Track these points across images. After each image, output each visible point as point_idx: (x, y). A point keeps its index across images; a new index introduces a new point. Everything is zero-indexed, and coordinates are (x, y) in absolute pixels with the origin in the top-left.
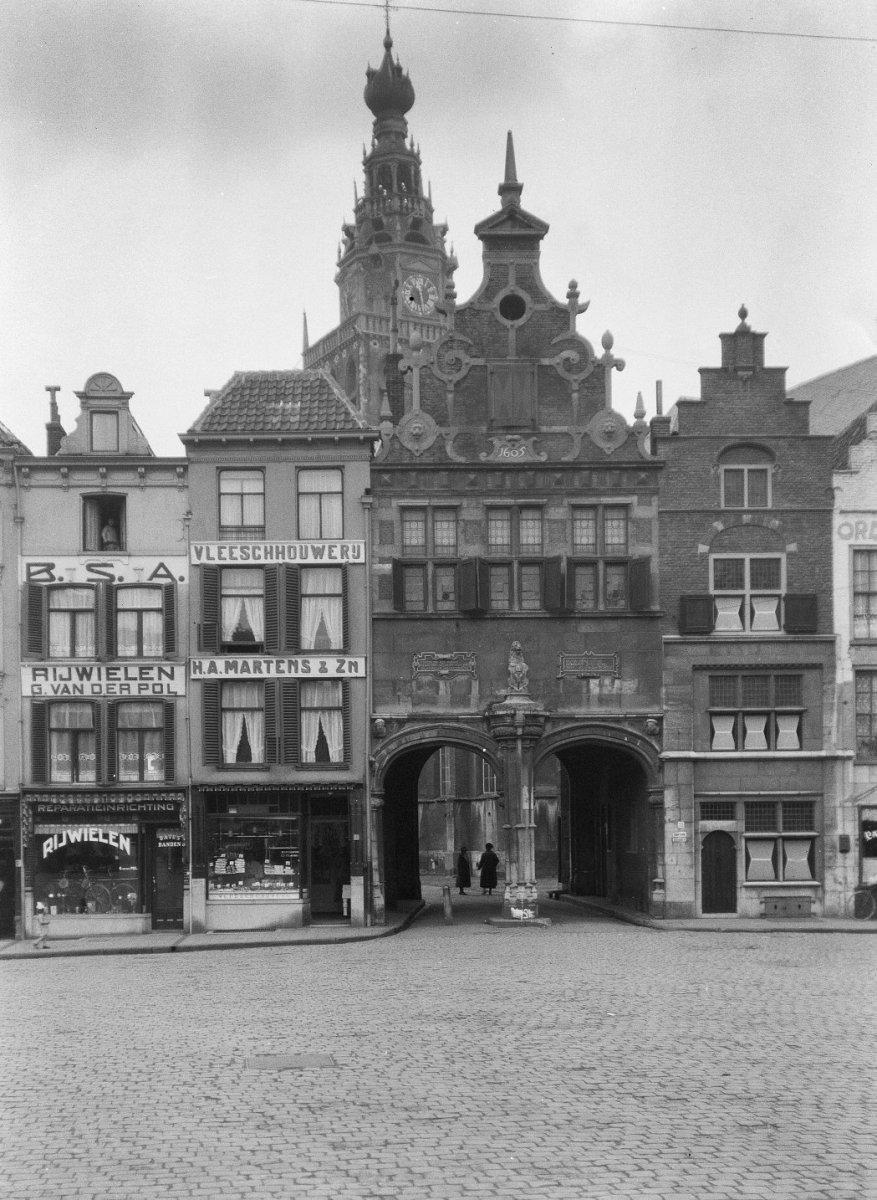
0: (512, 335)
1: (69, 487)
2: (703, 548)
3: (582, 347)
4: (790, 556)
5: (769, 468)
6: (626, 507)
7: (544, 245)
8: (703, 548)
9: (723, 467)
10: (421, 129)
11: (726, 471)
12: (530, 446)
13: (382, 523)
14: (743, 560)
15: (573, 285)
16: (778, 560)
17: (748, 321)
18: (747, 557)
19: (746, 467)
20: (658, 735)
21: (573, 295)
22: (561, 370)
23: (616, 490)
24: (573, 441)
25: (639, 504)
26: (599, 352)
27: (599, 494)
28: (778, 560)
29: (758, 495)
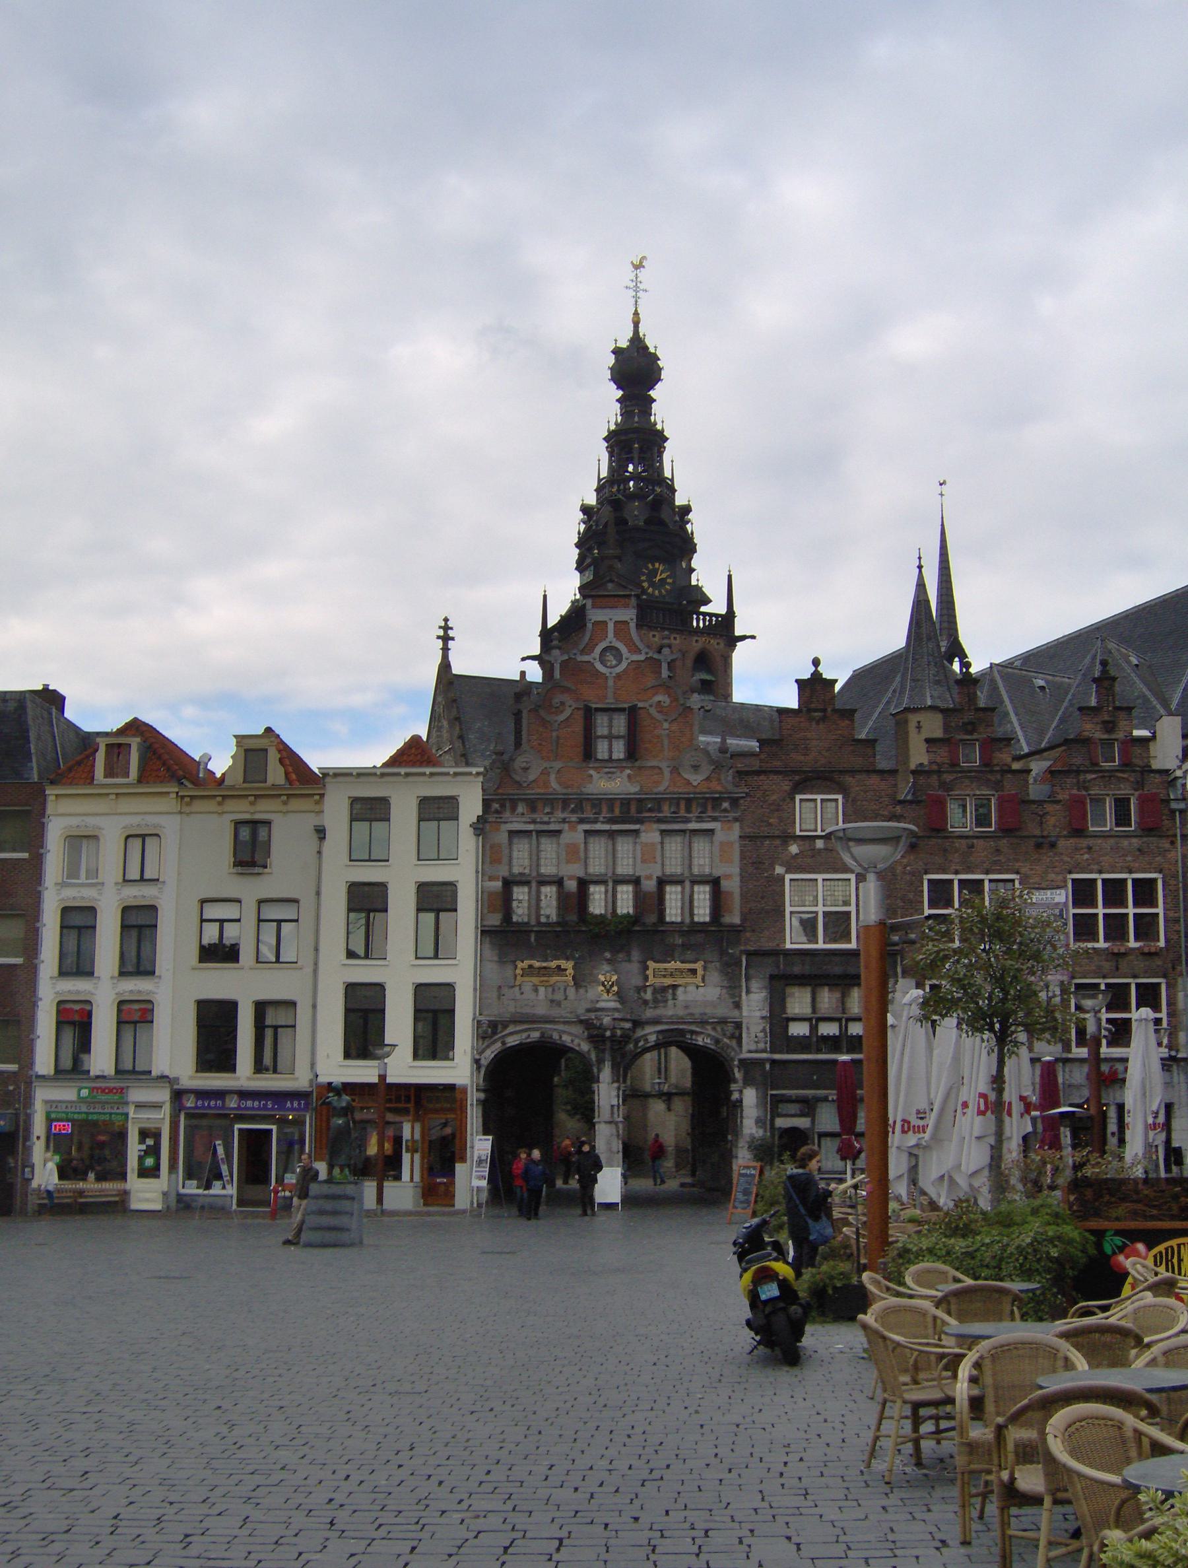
1: (223, 813)
2: (779, 870)
5: (840, 797)
8: (779, 870)
9: (798, 797)
11: (801, 800)
12: (626, 779)
17: (819, 669)
18: (820, 877)
19: (819, 797)
22: (653, 711)
23: (700, 819)
24: (662, 773)
25: (722, 829)
27: (688, 821)
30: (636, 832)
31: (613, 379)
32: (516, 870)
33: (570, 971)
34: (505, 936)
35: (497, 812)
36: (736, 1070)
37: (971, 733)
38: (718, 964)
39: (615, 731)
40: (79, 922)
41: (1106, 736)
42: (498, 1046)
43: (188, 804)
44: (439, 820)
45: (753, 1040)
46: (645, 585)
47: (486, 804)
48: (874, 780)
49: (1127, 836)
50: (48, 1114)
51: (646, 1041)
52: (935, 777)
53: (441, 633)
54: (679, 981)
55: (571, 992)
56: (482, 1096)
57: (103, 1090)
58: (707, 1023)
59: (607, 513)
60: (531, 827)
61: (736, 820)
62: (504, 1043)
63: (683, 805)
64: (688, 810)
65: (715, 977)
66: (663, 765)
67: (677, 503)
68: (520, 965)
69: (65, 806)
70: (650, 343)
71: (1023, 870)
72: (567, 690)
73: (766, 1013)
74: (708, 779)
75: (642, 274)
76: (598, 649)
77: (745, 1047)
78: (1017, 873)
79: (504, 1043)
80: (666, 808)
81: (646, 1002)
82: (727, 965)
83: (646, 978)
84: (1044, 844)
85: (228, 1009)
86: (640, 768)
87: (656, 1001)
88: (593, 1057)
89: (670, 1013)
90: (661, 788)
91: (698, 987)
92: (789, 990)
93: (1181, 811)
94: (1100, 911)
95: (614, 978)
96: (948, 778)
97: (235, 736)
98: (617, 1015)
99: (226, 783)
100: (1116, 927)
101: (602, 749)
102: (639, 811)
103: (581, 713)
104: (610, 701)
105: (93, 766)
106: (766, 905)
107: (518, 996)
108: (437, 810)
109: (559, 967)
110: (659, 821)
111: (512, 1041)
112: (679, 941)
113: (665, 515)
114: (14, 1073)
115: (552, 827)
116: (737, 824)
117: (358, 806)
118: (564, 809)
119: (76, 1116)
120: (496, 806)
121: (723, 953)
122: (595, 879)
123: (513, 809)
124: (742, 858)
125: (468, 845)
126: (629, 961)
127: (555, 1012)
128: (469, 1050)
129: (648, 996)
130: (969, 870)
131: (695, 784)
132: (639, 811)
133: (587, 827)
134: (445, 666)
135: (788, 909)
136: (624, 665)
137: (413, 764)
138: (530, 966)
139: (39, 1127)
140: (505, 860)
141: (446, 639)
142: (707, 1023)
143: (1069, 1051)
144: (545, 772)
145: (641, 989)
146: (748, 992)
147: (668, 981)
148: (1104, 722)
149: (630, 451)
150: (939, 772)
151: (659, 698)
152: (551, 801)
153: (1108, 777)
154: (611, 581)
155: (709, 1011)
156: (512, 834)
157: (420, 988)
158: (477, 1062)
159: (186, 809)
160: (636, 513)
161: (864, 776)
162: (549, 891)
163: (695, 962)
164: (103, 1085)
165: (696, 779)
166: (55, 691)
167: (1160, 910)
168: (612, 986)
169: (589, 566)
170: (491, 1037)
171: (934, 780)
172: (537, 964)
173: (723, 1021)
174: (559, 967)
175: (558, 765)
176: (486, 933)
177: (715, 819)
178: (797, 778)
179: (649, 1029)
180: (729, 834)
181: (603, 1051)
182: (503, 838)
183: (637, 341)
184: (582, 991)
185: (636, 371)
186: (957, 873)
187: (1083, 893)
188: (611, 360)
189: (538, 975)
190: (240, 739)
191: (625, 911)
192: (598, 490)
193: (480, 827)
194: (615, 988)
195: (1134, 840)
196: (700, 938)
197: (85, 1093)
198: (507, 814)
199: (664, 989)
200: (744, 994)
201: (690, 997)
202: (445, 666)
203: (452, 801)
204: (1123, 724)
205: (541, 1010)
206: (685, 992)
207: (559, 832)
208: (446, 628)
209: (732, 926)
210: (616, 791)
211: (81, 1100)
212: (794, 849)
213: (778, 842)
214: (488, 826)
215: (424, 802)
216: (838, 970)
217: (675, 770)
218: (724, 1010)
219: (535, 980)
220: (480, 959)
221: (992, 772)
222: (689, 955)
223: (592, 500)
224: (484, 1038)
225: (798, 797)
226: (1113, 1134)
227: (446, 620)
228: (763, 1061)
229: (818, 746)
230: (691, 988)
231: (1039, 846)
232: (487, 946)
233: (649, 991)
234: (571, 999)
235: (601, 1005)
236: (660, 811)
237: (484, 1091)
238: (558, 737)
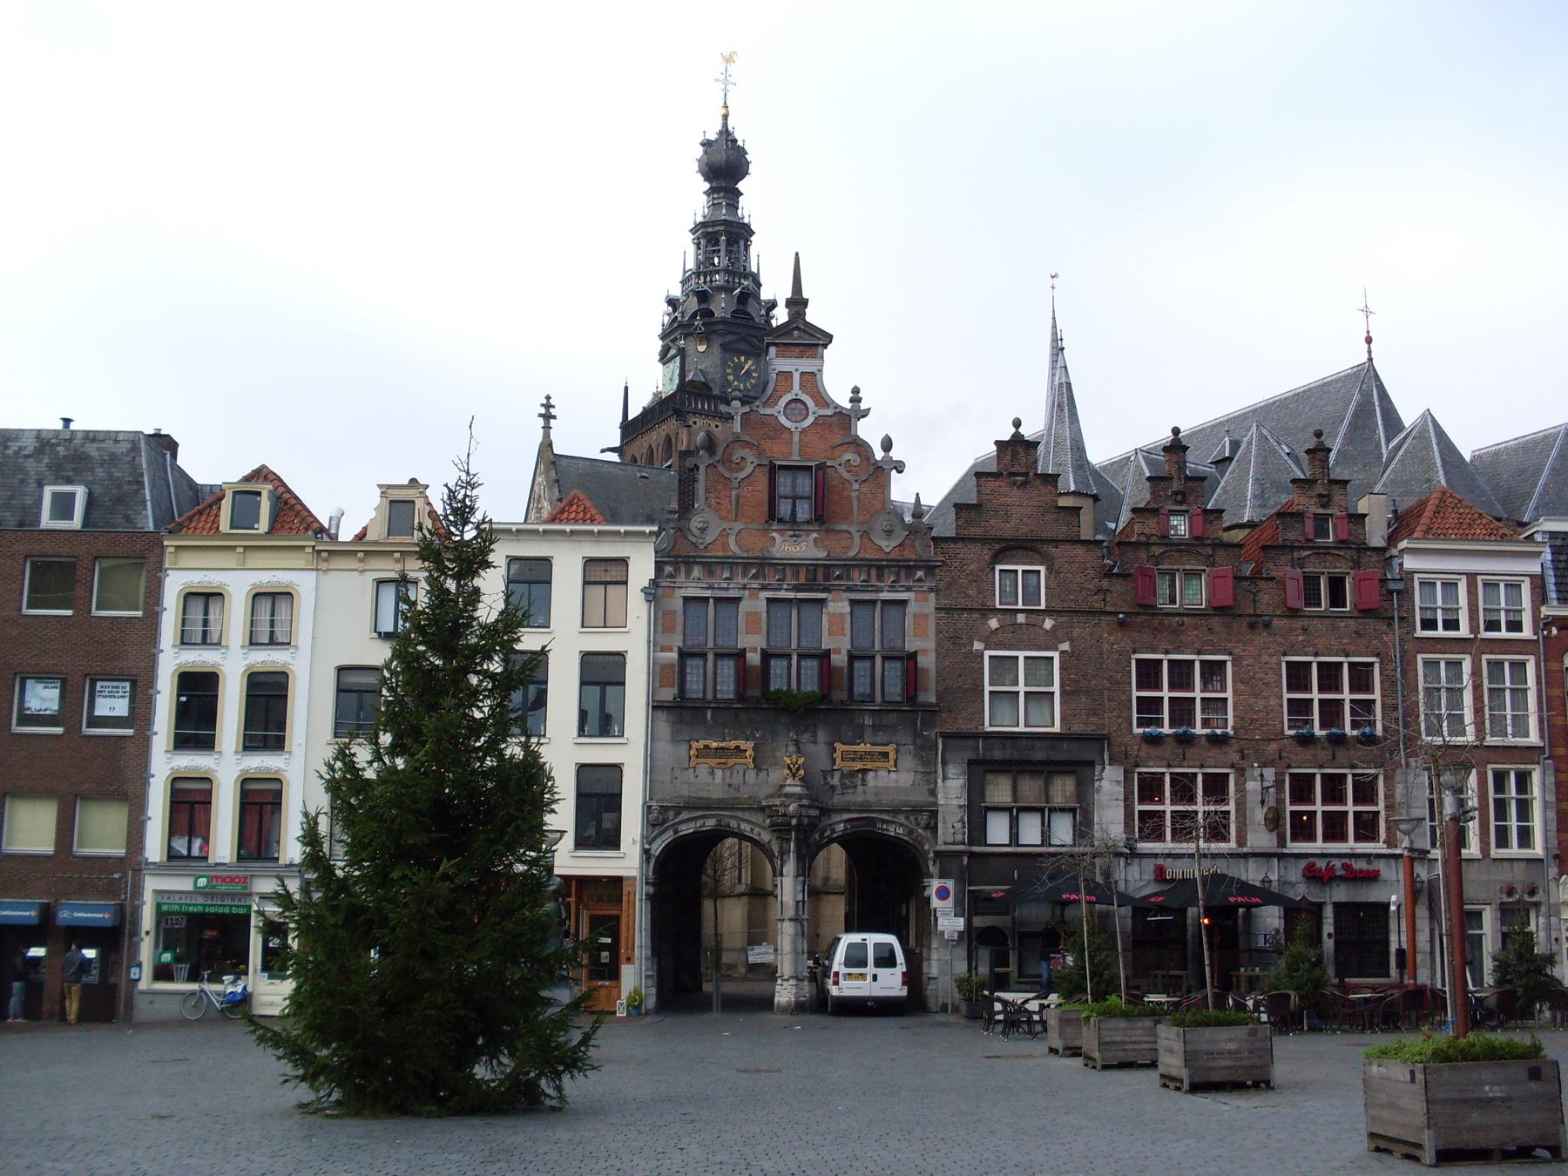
0: (796, 438)
2: (977, 646)
3: (862, 447)
4: (1062, 652)
5: (1042, 569)
7: (828, 353)
8: (977, 646)
9: (998, 567)
10: (754, 200)
13: (665, 613)
15: (856, 390)
18: (1021, 655)
19: (1020, 568)
20: (933, 828)
21: (856, 399)
22: (842, 470)
23: (892, 589)
26: (879, 455)
27: (880, 590)
29: (1031, 595)
30: (822, 602)
31: (700, 171)
32: (689, 643)
34: (679, 709)
35: (671, 576)
36: (930, 863)
37: (1180, 503)
39: (799, 491)
40: (198, 692)
41: (1321, 511)
42: (668, 837)
43: (326, 560)
44: (606, 583)
45: (950, 830)
46: (731, 378)
47: (659, 566)
48: (1079, 551)
49: (1342, 617)
50: (158, 905)
51: (833, 831)
53: (543, 411)
55: (751, 774)
56: (651, 890)
57: (224, 879)
58: (900, 811)
59: (693, 304)
60: (708, 593)
61: (931, 590)
63: (874, 572)
64: (880, 578)
65: (908, 761)
66: (853, 529)
67: (763, 297)
68: (695, 745)
69: (187, 559)
70: (739, 136)
71: (1236, 651)
72: (748, 444)
73: (963, 802)
75: (732, 68)
76: (783, 402)
77: (940, 840)
78: (1230, 654)
79: (676, 832)
80: (855, 574)
81: (833, 788)
82: (922, 748)
83: (834, 761)
84: (1258, 623)
85: (1521, 845)
86: (828, 531)
87: (843, 786)
88: (775, 848)
89: (860, 799)
90: (852, 554)
92: (990, 777)
93: (1399, 592)
94: (1315, 695)
95: (801, 761)
96: (1157, 550)
97: (380, 486)
98: (805, 802)
99: (367, 538)
100: (1331, 712)
101: (784, 509)
102: (827, 578)
103: (766, 470)
104: (795, 459)
105: (217, 516)
106: (963, 687)
108: (604, 575)
110: (849, 589)
111: (686, 829)
112: (868, 721)
113: (751, 308)
114: (121, 859)
115: (732, 594)
117: (515, 567)
118: (744, 575)
119: (191, 909)
120: (668, 569)
121: (917, 735)
122: (777, 651)
123: (688, 574)
124: (938, 631)
125: (638, 610)
126: (815, 742)
128: (638, 839)
129: (836, 781)
130: (1179, 650)
132: (827, 578)
133: (770, 594)
134: (547, 445)
135: (987, 688)
136: (810, 420)
137: (576, 521)
138: (706, 747)
139: (147, 920)
140: (679, 628)
141: (548, 417)
142: (900, 811)
143: (1284, 846)
144: (724, 533)
145: (825, 773)
146: (945, 778)
147: (859, 765)
148: (1319, 495)
149: (717, 243)
150: (1148, 545)
151: (848, 456)
152: (731, 563)
153: (1322, 552)
154: (797, 328)
155: (903, 798)
156: (686, 599)
157: (583, 769)
158: (646, 852)
159: (324, 566)
160: (721, 306)
161: (1068, 546)
162: (727, 668)
164: (224, 874)
165: (888, 545)
166: (167, 436)
167: (1377, 695)
169: (673, 357)
171: (1143, 555)
172: (714, 745)
173: (916, 810)
175: (738, 526)
176: (656, 707)
177: (909, 589)
178: (997, 547)
179: (836, 818)
180: (921, 605)
181: (788, 840)
182: (678, 604)
183: (726, 133)
184: (763, 774)
185: (725, 167)
186: (1167, 652)
187: (1298, 676)
188: (699, 152)
190: (385, 489)
191: (809, 688)
192: (684, 282)
193: (653, 593)
194: (802, 772)
195: (1351, 622)
196: (892, 718)
197: (202, 882)
198: (682, 578)
199: (853, 774)
200: (940, 781)
201: (881, 783)
202: (547, 445)
203: (623, 562)
204: (1338, 497)
205: (717, 794)
207: (737, 600)
208: (548, 406)
209: (930, 705)
210: (800, 555)
211: (197, 891)
212: (994, 623)
214: (660, 591)
215: (590, 562)
216: (1039, 755)
217: (865, 534)
218: (920, 797)
219: (713, 762)
220: (652, 736)
221: (1202, 545)
222: (881, 738)
223: (677, 291)
224: (654, 825)
226: (1330, 935)
227: (548, 398)
228: (960, 854)
229: (1018, 510)
230: (883, 773)
231: (1252, 626)
233: (837, 775)
235: (788, 790)
236: (849, 578)
237: (654, 885)
238: (738, 496)
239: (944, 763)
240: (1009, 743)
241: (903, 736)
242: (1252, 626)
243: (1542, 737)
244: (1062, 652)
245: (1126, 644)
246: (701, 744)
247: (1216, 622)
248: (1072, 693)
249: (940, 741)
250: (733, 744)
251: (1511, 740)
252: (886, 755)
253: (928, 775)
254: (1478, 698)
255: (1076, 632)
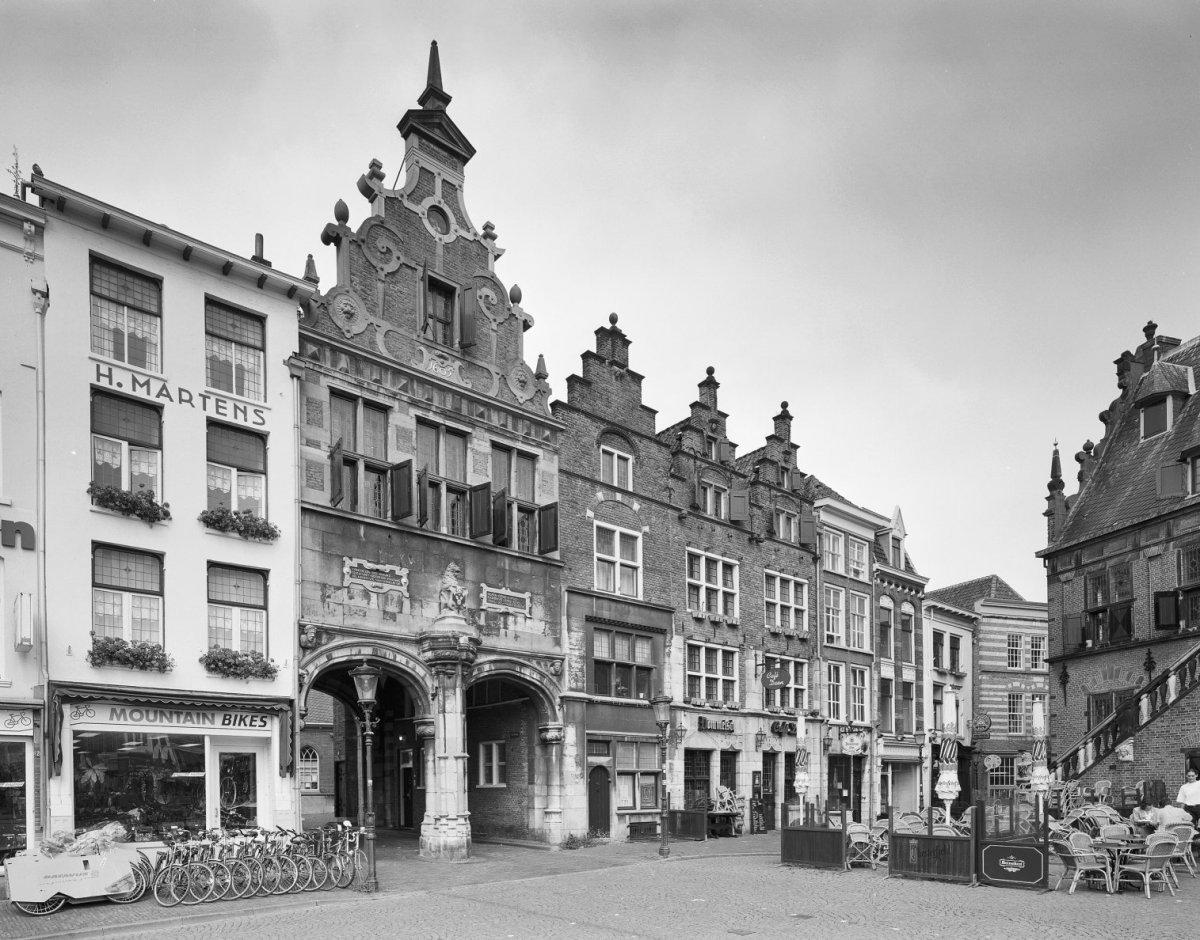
4: (645, 534)
6: (533, 458)
9: (603, 447)
14: (614, 532)
16: (635, 538)
23: (526, 440)
27: (514, 438)
28: (635, 538)
33: (404, 580)
38: (542, 598)
52: (692, 461)
54: (511, 610)
62: (330, 658)
63: (510, 420)
64: (515, 427)
65: (539, 611)
74: (531, 400)
79: (330, 658)
83: (479, 601)
91: (526, 618)
92: (597, 636)
107: (347, 601)
109: (392, 572)
116: (556, 457)
121: (546, 587)
127: (389, 628)
131: (521, 401)
135: (596, 555)
138: (360, 566)
147: (503, 609)
163: (523, 592)
168: (463, 601)
170: (313, 649)
174: (392, 572)
177: (539, 445)
189: (369, 578)
196: (525, 567)
200: (565, 632)
206: (516, 623)
213: (588, 485)
218: (546, 647)
219: (369, 584)
222: (518, 584)
225: (603, 447)
232: (308, 532)
234: (424, 614)
239: (569, 617)
240: (613, 605)
241: (537, 585)
242: (750, 540)
243: (872, 649)
244: (645, 534)
245: (682, 537)
246: (355, 562)
247: (732, 532)
248: (652, 570)
249: (566, 594)
250: (388, 568)
251: (856, 649)
252: (522, 601)
253: (553, 625)
254: (847, 619)
255: (654, 519)
